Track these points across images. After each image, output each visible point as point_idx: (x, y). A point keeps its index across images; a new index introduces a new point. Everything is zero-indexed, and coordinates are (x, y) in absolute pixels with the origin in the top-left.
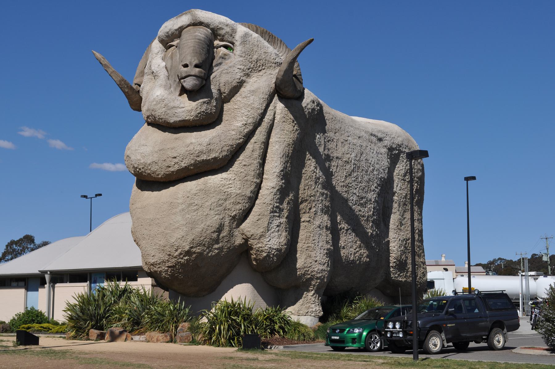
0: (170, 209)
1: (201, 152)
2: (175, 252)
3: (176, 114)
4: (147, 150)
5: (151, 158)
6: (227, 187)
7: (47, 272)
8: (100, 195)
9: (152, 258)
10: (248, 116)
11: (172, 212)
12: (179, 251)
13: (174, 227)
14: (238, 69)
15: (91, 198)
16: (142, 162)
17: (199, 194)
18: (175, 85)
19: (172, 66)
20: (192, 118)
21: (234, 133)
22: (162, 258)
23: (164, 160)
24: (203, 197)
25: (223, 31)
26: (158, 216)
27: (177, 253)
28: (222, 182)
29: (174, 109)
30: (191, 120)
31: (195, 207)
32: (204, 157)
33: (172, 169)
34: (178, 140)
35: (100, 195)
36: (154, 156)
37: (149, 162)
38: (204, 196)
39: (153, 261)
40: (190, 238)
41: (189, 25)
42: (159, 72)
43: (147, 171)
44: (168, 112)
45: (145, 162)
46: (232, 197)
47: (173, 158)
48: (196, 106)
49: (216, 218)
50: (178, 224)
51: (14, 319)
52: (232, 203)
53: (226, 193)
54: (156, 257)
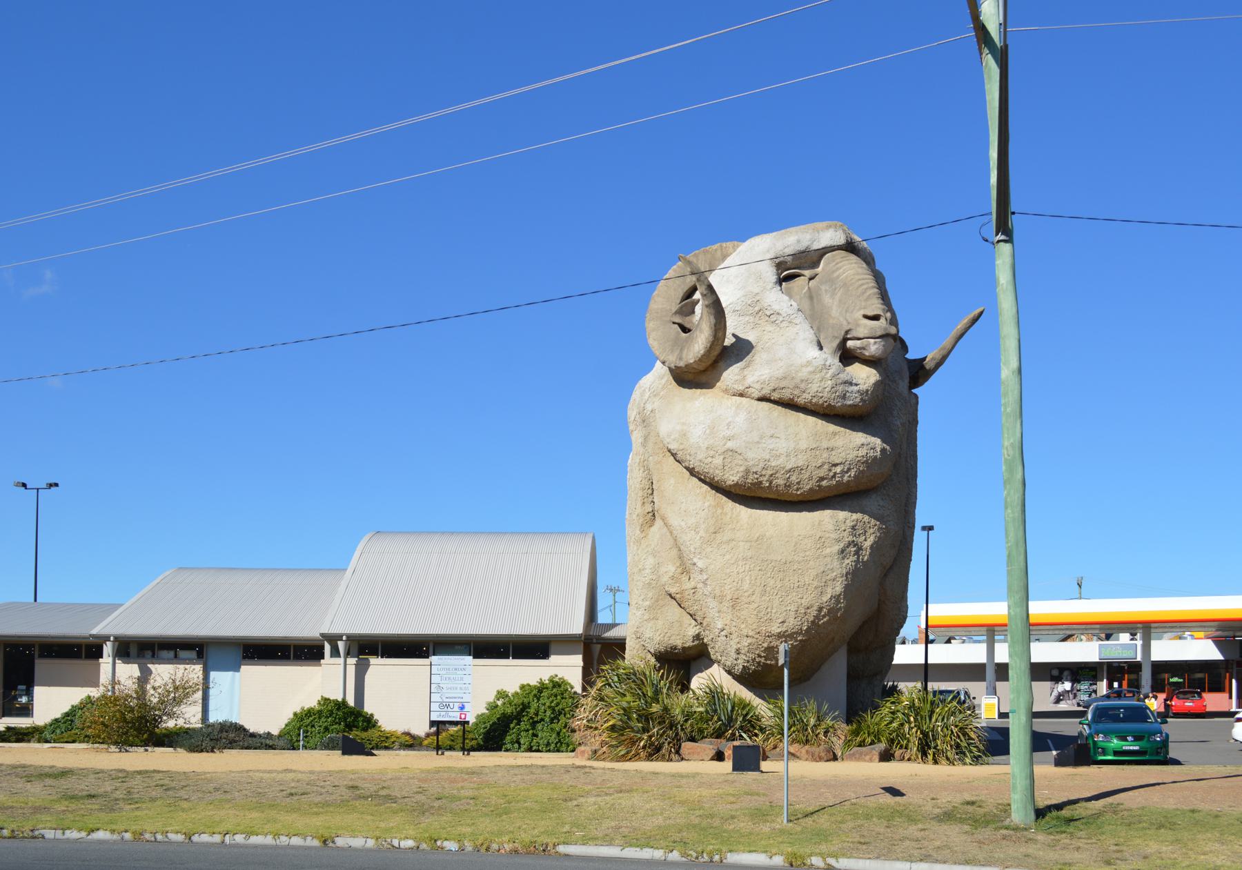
0: (819, 548)
4: (783, 445)
5: (793, 460)
7: (342, 636)
8: (56, 485)
11: (823, 553)
13: (829, 577)
15: (38, 489)
26: (796, 558)
34: (837, 437)
35: (56, 485)
39: (779, 630)
45: (782, 466)
50: (835, 574)
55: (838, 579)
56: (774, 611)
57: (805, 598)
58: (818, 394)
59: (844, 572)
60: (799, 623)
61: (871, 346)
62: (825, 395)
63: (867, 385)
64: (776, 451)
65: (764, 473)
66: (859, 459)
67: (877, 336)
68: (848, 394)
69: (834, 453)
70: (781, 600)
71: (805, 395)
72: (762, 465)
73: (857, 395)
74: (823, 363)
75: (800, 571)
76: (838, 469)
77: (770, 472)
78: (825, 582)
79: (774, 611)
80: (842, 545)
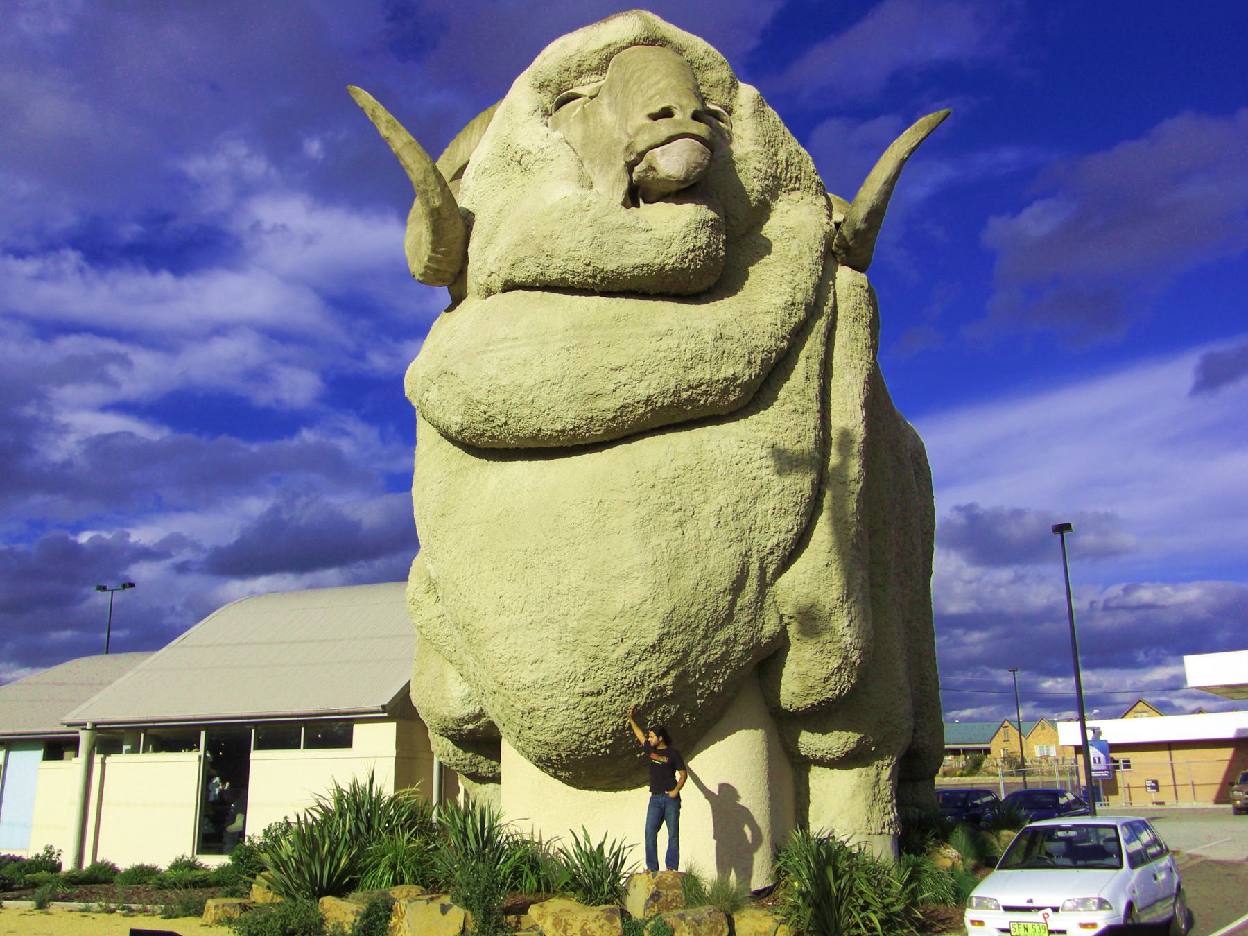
1: (696, 360)
2: (613, 647)
3: (627, 247)
6: (757, 464)
9: (530, 667)
10: (793, 285)
11: (605, 529)
12: (628, 644)
14: (756, 171)
16: (503, 383)
17: (684, 480)
18: (611, 177)
19: (586, 137)
20: (671, 261)
21: (769, 320)
22: (566, 669)
23: (581, 375)
24: (694, 489)
25: (714, 74)
27: (621, 651)
28: (742, 451)
29: (620, 231)
30: (667, 268)
31: (677, 516)
32: (704, 373)
33: (601, 404)
36: (548, 363)
37: (529, 382)
38: (698, 486)
39: (534, 677)
40: (665, 606)
41: (634, 43)
42: (550, 149)
43: (515, 411)
44: (604, 238)
45: (517, 382)
46: (771, 493)
47: (612, 370)
48: (684, 230)
49: (732, 550)
50: (628, 565)
51: (578, 901)
52: (770, 512)
53: (758, 482)
54: (544, 666)
55: (636, 574)
56: (519, 641)
57: (572, 613)
58: (572, 253)
59: (650, 560)
60: (568, 662)
61: (658, 158)
62: (584, 252)
63: (670, 230)
64: (509, 359)
65: (491, 399)
66: (663, 354)
67: (664, 139)
68: (627, 247)
69: (612, 350)
70: (530, 619)
71: (557, 262)
72: (486, 386)
73: (648, 247)
74: (578, 201)
75: (561, 565)
76: (622, 377)
77: (500, 397)
78: (609, 582)
79: (519, 641)
80: (643, 512)
